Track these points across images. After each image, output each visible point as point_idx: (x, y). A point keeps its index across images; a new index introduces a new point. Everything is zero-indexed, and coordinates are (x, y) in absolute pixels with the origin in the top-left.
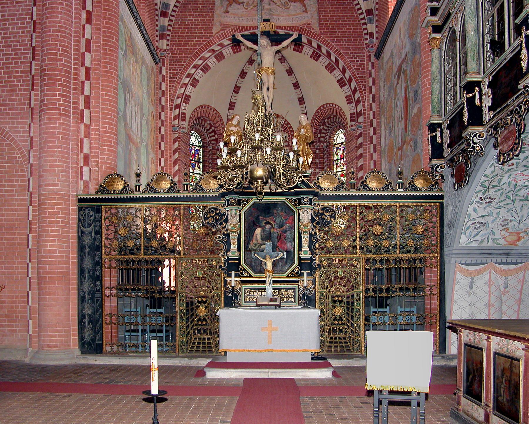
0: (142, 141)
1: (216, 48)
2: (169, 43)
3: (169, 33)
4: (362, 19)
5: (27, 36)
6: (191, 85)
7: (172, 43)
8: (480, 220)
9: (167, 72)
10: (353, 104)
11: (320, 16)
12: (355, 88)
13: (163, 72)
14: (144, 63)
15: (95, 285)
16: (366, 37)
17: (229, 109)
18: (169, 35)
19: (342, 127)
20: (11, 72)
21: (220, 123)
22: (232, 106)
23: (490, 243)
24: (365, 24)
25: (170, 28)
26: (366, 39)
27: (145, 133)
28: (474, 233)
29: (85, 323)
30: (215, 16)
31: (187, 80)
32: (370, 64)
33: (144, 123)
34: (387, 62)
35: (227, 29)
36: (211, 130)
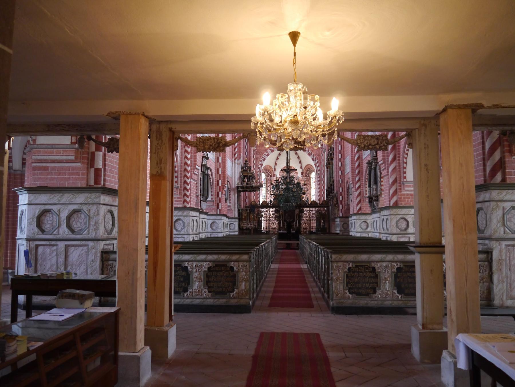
10: (317, 167)
13: (255, 157)
17: (275, 165)
21: (272, 170)
22: (276, 164)
31: (262, 159)
32: (322, 154)
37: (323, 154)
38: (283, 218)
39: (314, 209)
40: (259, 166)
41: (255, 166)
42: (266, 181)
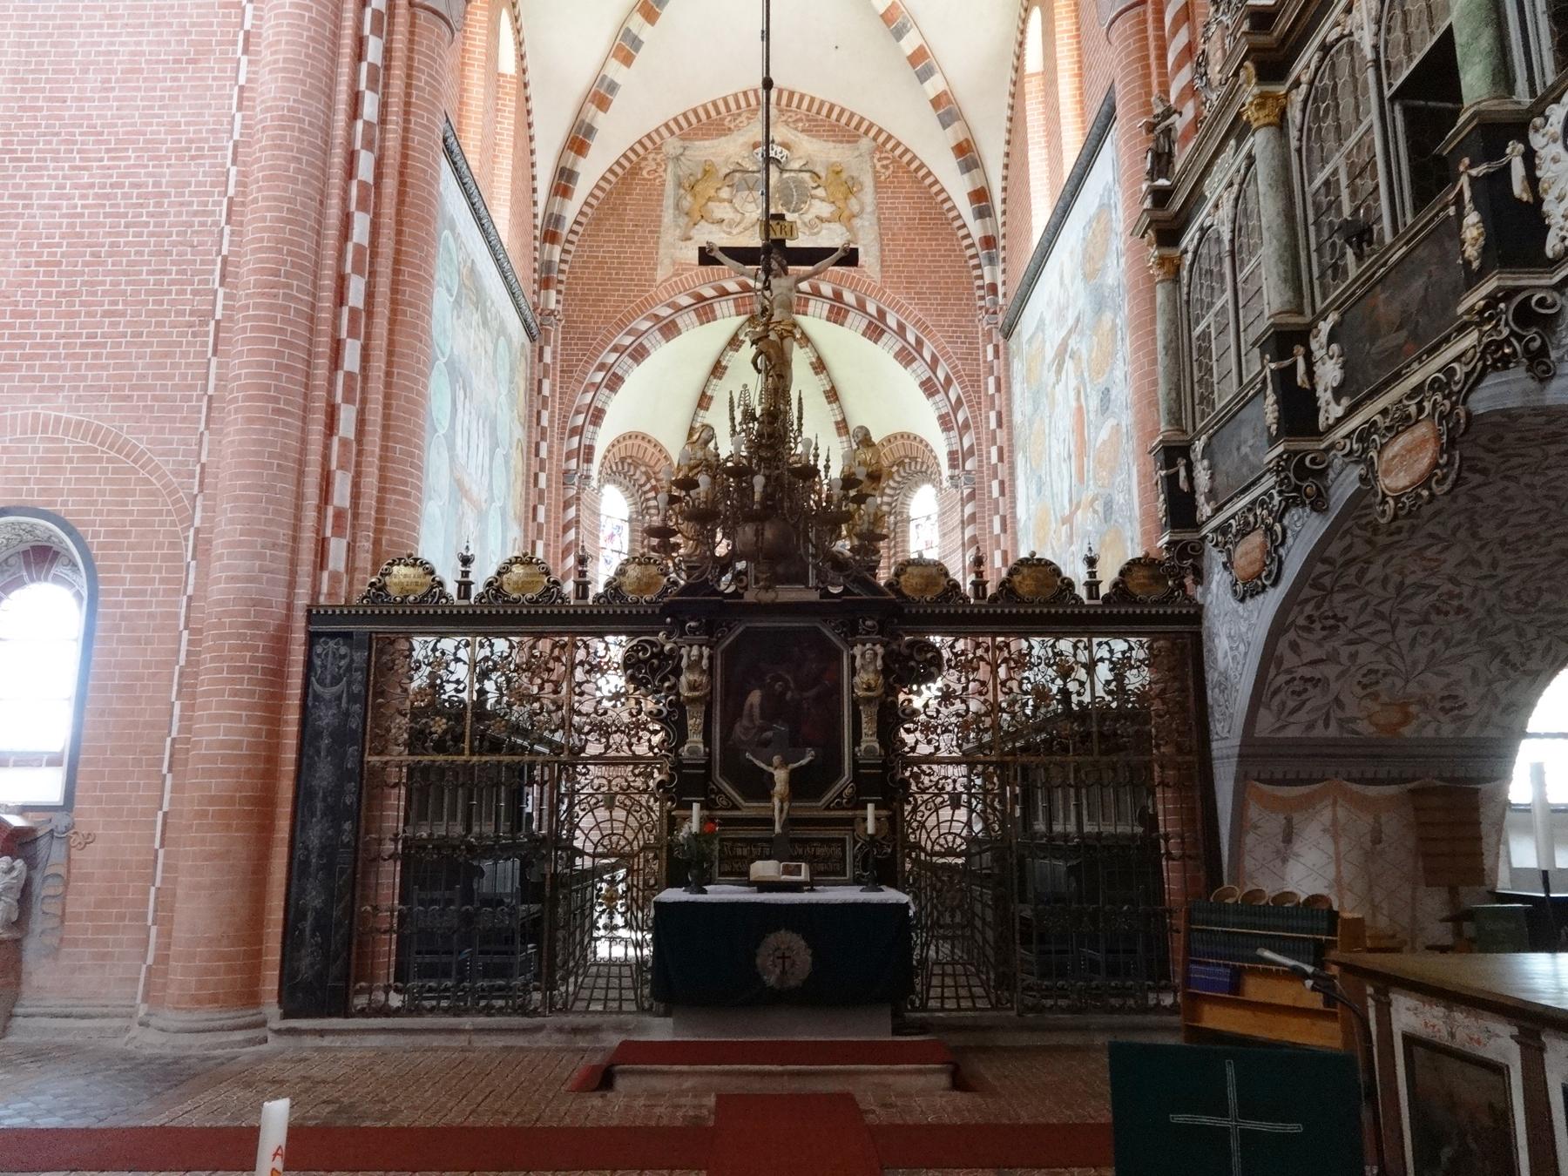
0: (491, 499)
1: (664, 312)
2: (561, 298)
3: (563, 277)
4: (972, 257)
5: (211, 233)
6: (607, 386)
7: (568, 297)
8: (1307, 672)
9: (554, 358)
10: (954, 433)
11: (882, 250)
12: (959, 399)
13: (548, 358)
14: (502, 331)
15: (340, 832)
16: (981, 293)
18: (561, 282)
19: (930, 480)
20: (167, 313)
23: (1333, 731)
24: (978, 266)
25: (565, 267)
26: (982, 298)
27: (500, 482)
28: (1291, 704)
29: (302, 932)
30: (662, 245)
31: (599, 377)
32: (990, 349)
33: (499, 459)
34: (1030, 341)
35: (687, 274)
36: (648, 487)
37: (996, 348)
38: (707, 741)
39: (1035, 641)
40: (580, 420)
41: (545, 415)
42: (632, 541)
